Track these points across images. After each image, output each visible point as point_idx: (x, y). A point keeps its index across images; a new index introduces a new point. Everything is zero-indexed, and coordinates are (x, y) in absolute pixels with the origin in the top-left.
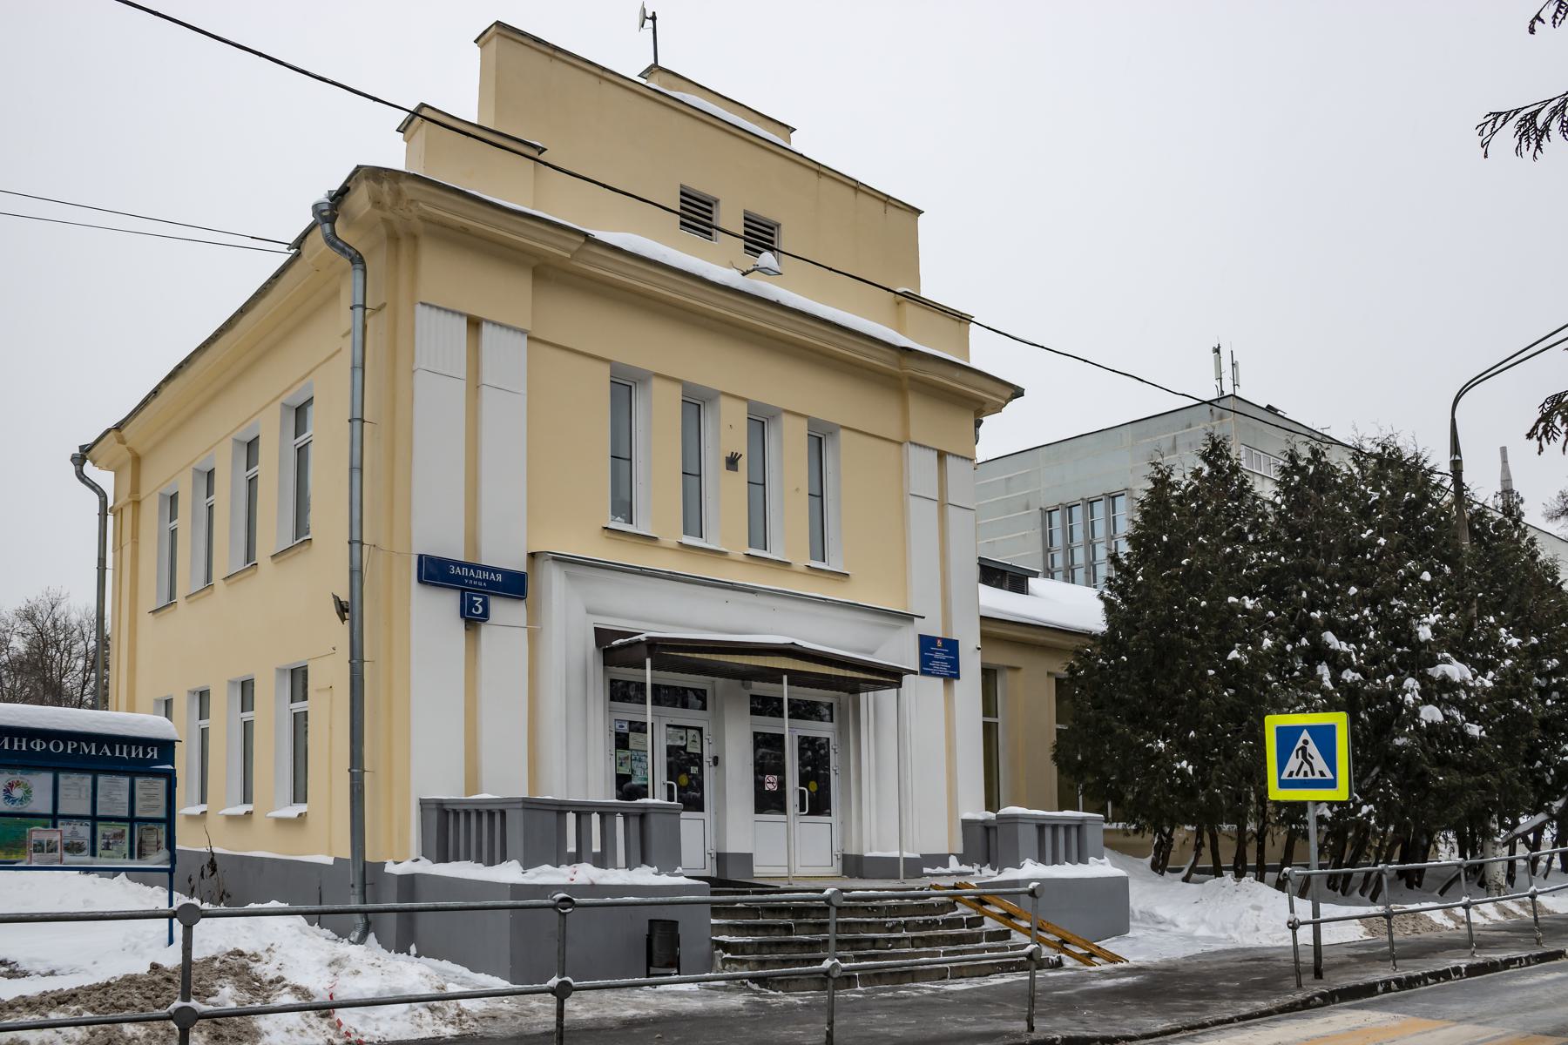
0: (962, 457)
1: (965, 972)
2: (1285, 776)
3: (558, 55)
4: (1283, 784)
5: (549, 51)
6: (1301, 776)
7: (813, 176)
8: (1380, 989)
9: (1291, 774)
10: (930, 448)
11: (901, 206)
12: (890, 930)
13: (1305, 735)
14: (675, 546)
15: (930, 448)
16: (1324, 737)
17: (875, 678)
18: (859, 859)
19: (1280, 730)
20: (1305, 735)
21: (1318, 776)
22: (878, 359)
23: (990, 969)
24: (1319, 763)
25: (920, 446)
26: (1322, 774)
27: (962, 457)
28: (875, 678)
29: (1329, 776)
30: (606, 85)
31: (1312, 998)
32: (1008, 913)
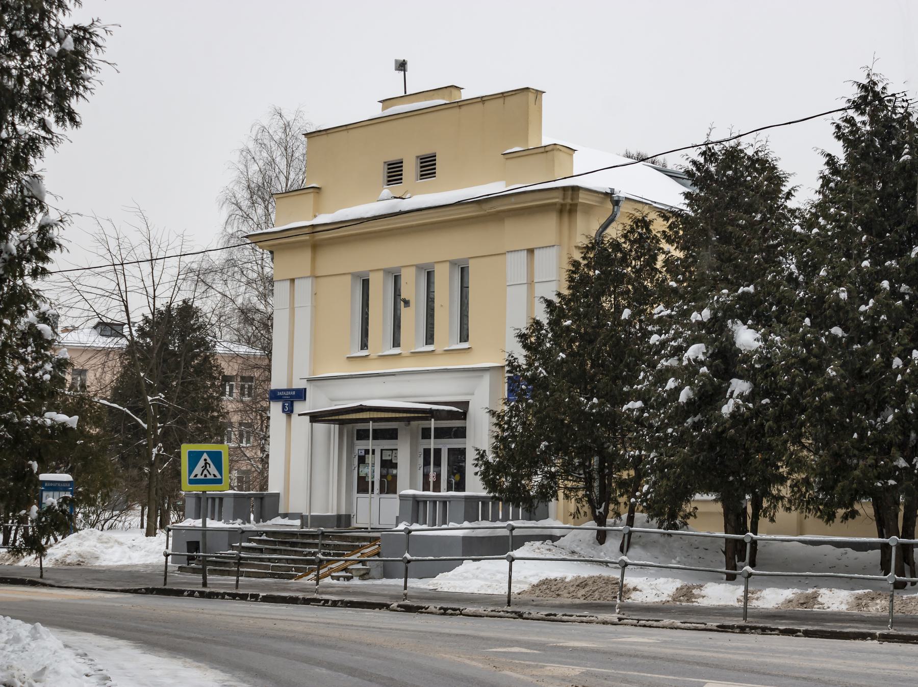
0: (546, 247)
1: (251, 575)
2: (192, 477)
3: (349, 127)
4: (191, 482)
5: (324, 133)
6: (203, 477)
7: (457, 110)
8: (330, 603)
9: (196, 476)
10: (521, 250)
11: (514, 93)
12: (305, 555)
13: (205, 456)
14: (408, 354)
15: (521, 250)
16: (194, 457)
17: (416, 415)
18: (853, 517)
19: (190, 453)
20: (205, 456)
21: (212, 477)
22: (470, 212)
23: (264, 575)
24: (213, 469)
25: (515, 251)
26: (215, 476)
27: (546, 247)
28: (416, 415)
29: (219, 477)
30: (351, 131)
31: (141, 589)
32: (905, 561)
